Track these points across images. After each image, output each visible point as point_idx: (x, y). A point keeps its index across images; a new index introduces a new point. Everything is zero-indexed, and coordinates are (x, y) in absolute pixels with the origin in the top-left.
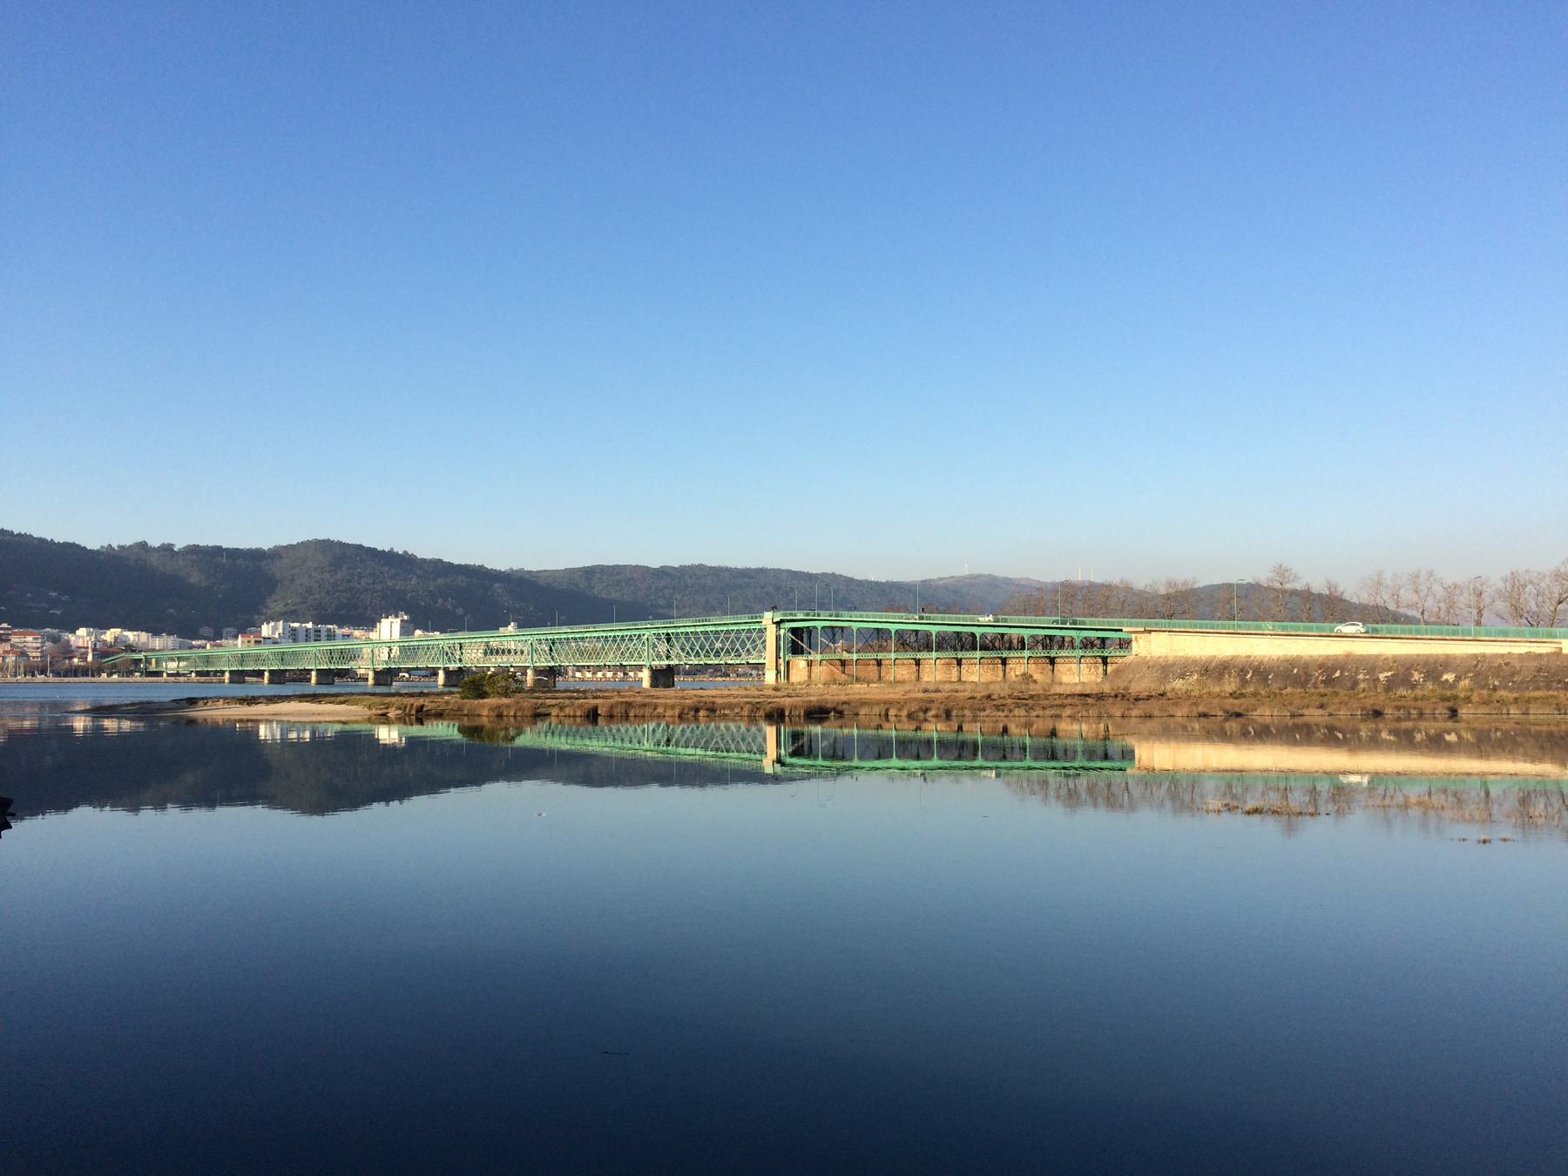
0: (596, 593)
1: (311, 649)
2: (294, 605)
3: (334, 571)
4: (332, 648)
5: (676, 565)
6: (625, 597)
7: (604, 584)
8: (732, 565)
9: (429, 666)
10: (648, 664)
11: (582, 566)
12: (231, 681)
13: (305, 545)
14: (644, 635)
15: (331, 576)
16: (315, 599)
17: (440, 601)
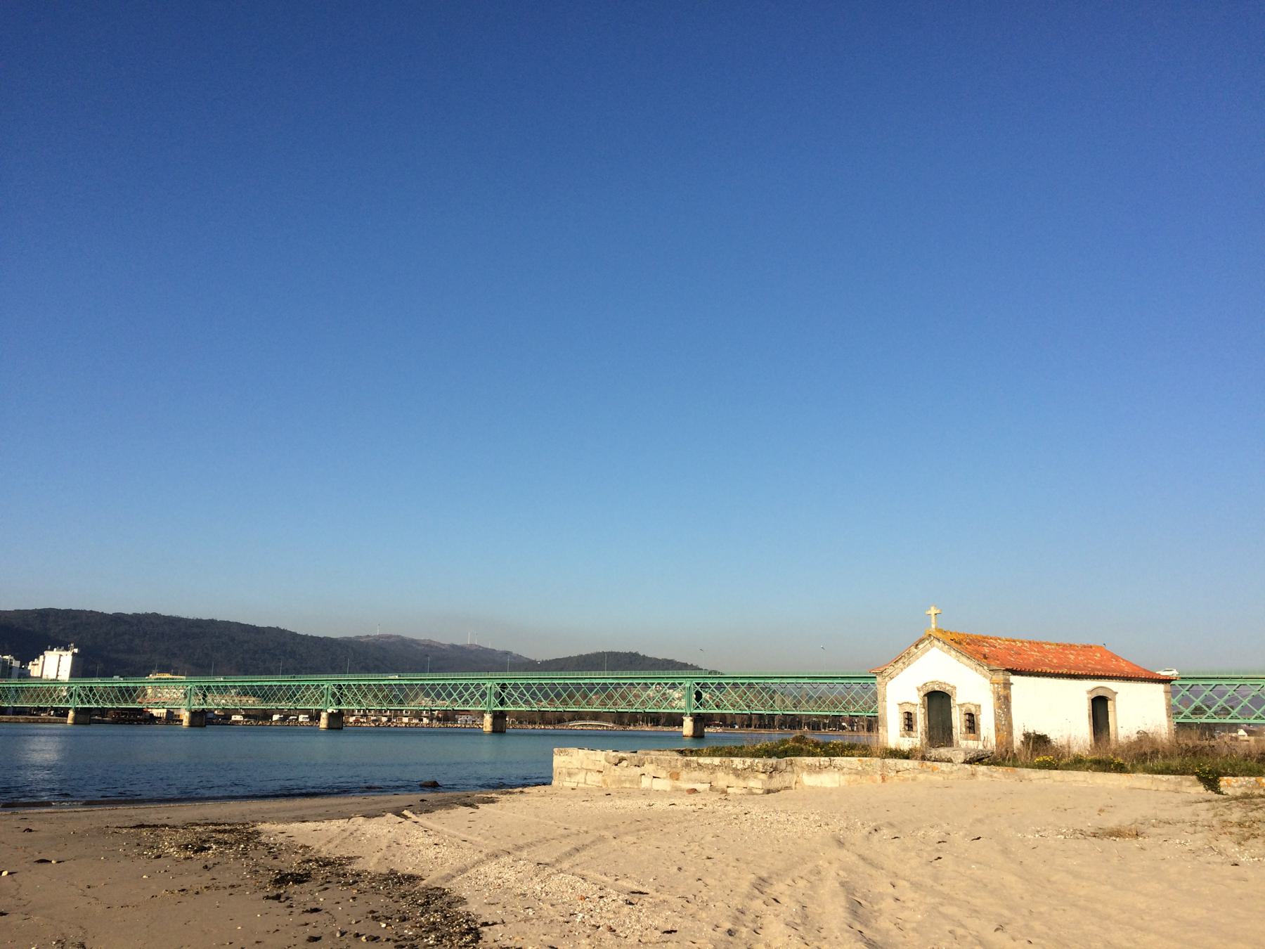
5: (130, 613)
14: (72, 687)
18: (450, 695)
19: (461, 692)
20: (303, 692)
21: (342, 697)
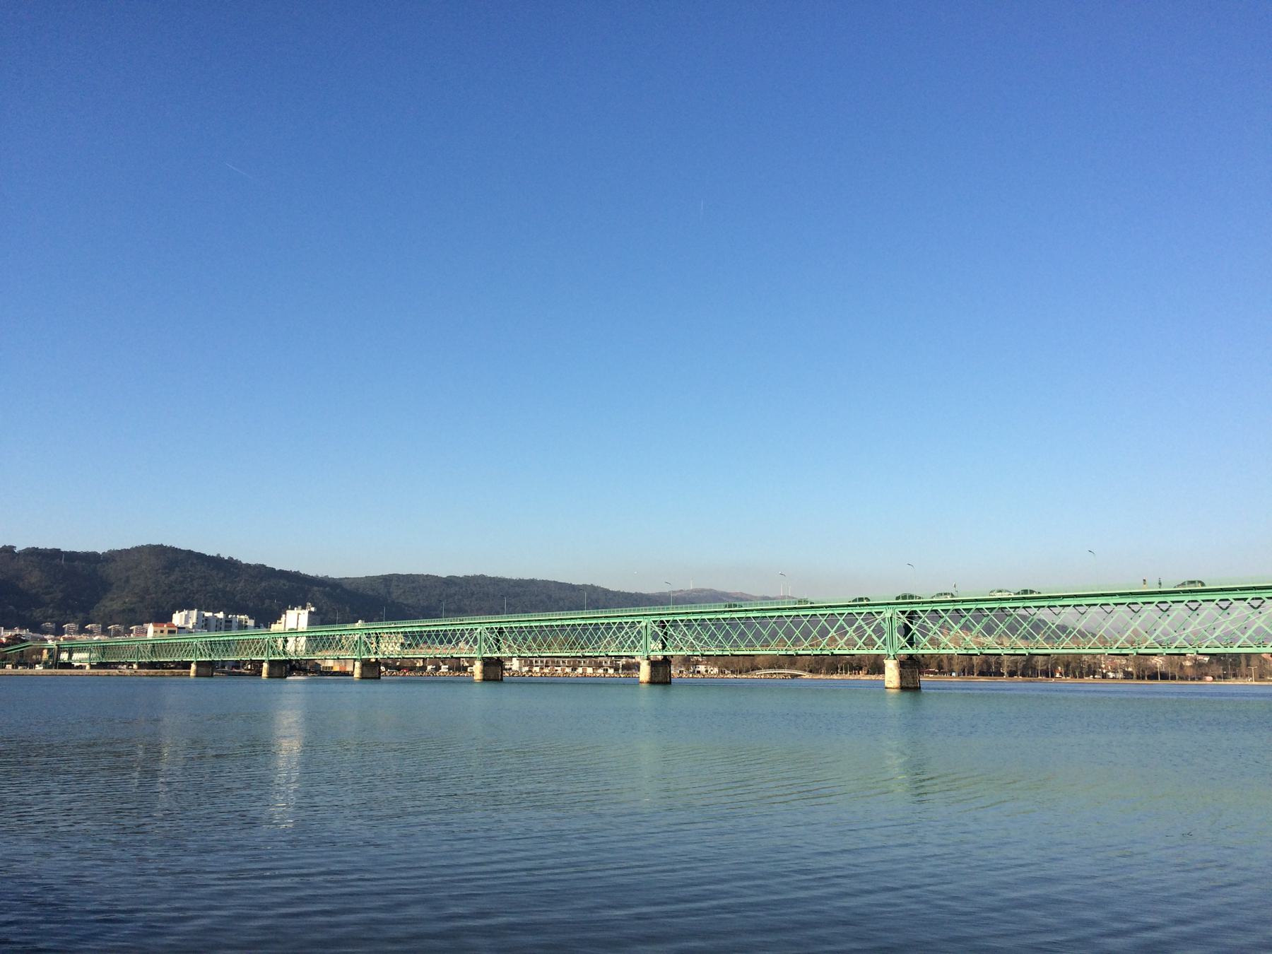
0: (394, 597)
1: (191, 640)
2: (131, 604)
3: (168, 573)
4: (212, 639)
6: (421, 602)
7: (402, 590)
8: (508, 577)
9: (253, 659)
10: (892, 654)
11: (381, 574)
12: (198, 675)
13: (138, 550)
15: (166, 577)
16: (152, 599)
17: (267, 602)
18: (742, 635)
19: (841, 627)
20: (614, 633)
21: (667, 640)
